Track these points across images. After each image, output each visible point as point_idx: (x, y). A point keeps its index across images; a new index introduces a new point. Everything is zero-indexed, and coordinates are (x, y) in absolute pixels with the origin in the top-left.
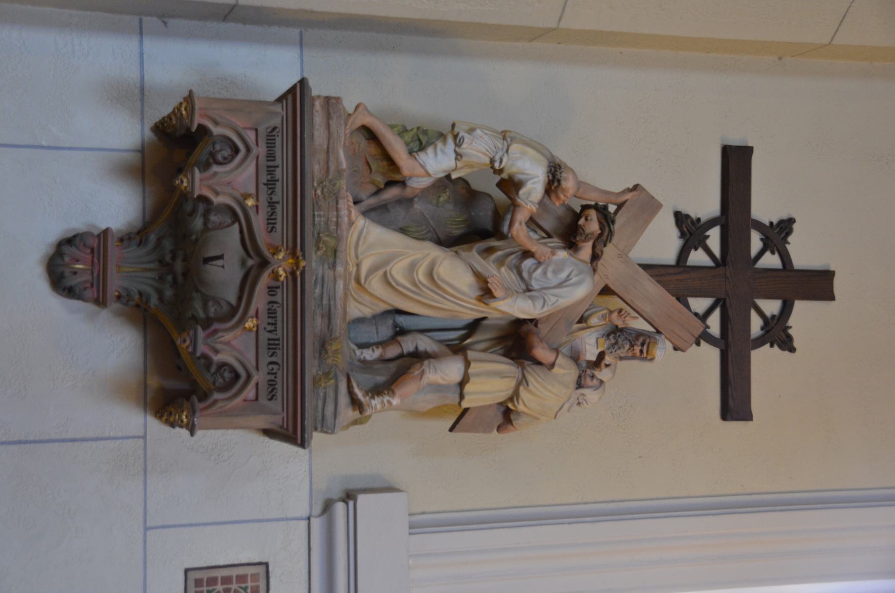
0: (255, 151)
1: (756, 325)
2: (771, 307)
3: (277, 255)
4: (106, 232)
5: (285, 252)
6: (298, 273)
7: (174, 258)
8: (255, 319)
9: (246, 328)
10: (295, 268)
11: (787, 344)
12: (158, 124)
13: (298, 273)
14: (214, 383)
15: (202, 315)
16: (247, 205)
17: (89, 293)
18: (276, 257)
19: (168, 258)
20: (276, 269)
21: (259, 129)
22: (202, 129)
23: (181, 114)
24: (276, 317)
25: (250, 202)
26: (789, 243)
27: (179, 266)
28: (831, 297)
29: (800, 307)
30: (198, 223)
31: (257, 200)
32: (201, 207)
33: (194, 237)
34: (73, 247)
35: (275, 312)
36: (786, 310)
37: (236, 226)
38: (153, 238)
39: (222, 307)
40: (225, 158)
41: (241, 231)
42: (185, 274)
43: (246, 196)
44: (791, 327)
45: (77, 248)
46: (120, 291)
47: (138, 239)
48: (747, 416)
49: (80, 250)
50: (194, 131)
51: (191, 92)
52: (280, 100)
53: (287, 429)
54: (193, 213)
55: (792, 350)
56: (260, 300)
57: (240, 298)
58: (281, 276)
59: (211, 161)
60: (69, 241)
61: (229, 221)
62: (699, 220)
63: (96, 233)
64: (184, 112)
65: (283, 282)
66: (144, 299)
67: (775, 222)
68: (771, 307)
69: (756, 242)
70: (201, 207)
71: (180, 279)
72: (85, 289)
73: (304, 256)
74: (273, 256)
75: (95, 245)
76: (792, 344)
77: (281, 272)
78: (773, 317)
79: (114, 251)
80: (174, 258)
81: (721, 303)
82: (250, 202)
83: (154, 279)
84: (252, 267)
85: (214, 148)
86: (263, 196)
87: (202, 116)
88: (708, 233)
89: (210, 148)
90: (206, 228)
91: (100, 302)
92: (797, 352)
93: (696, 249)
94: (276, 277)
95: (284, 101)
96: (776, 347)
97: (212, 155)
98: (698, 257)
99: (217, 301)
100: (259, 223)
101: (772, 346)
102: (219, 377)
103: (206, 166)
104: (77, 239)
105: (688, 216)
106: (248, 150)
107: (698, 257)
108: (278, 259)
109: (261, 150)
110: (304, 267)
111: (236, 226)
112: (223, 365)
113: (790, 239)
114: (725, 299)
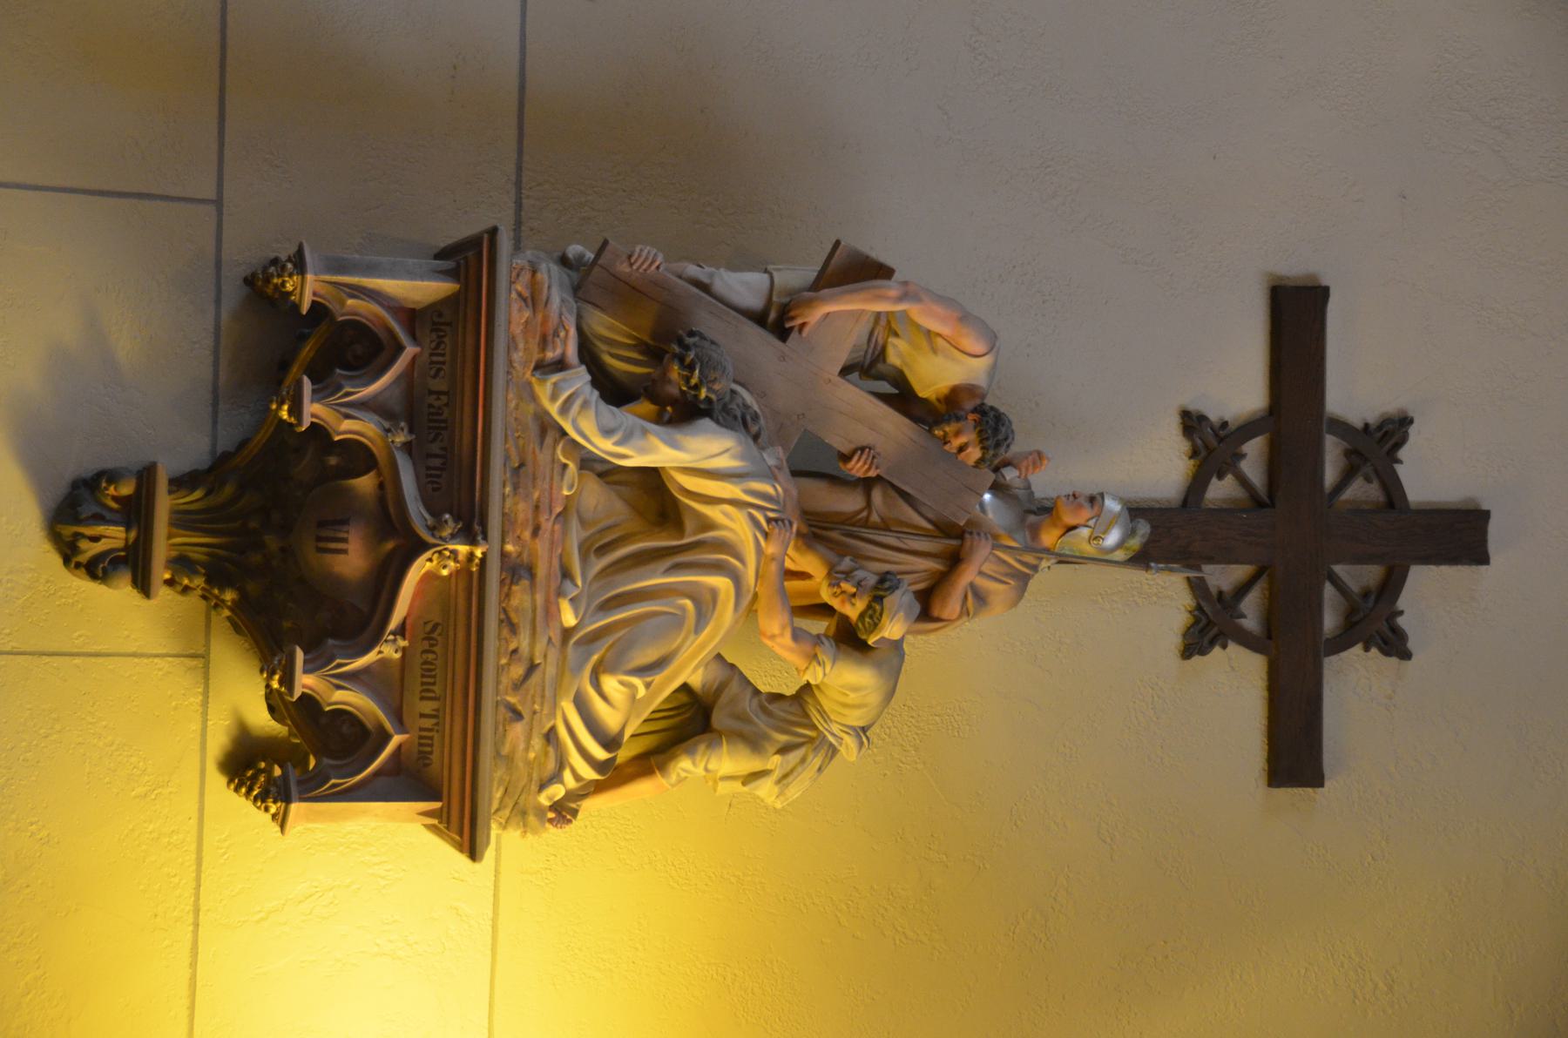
11: (1394, 644)
28: (1481, 558)
31: (411, 431)
44: (1401, 613)
50: (304, 313)
55: (1406, 655)
62: (1225, 424)
76: (1405, 645)
92: (1413, 659)
93: (1220, 477)
96: (1374, 651)
98: (1221, 490)
101: (1367, 649)
105: (1202, 418)
113: (1403, 453)
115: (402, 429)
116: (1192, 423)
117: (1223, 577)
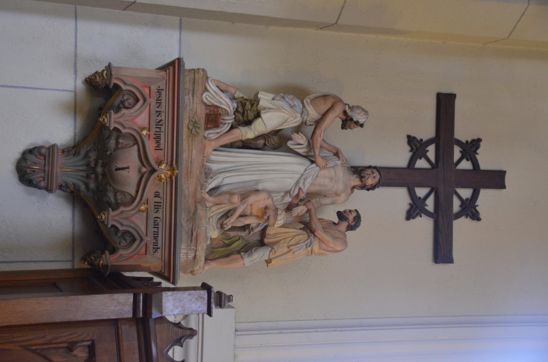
0: (149, 100)
1: (456, 205)
2: (466, 193)
3: (161, 166)
4: (54, 146)
5: (165, 164)
6: (174, 178)
7: (96, 164)
8: (146, 205)
9: (140, 210)
10: (172, 174)
11: (475, 216)
12: (87, 79)
13: (174, 178)
14: (120, 243)
15: (113, 200)
16: (143, 134)
17: (43, 184)
18: (160, 167)
19: (92, 165)
20: (160, 174)
21: (151, 87)
22: (117, 86)
23: (104, 77)
24: (158, 228)
25: (145, 132)
26: (478, 154)
27: (99, 170)
28: (503, 186)
29: (484, 194)
30: (112, 143)
32: (114, 134)
33: (108, 153)
34: (33, 155)
35: (158, 224)
36: (475, 195)
37: (135, 147)
38: (83, 152)
39: (126, 196)
40: (130, 104)
41: (139, 150)
42: (104, 175)
43: (144, 129)
44: (478, 206)
45: (36, 156)
46: (62, 184)
47: (73, 151)
48: (449, 260)
49: (38, 158)
51: (110, 65)
52: (164, 68)
53: (164, 273)
54: (109, 137)
55: (479, 219)
56: (149, 193)
57: (137, 192)
58: (163, 179)
59: (121, 106)
60: (30, 151)
61: (131, 143)
62: (422, 140)
63: (47, 146)
64: (105, 76)
65: (164, 183)
66: (76, 188)
67: (469, 141)
68: (466, 193)
69: (457, 153)
70: (114, 134)
71: (100, 178)
72: (40, 181)
73: (177, 167)
74: (158, 167)
75: (47, 155)
77: (163, 176)
78: (467, 199)
79: (60, 160)
80: (96, 164)
81: (435, 191)
82: (145, 132)
83: (83, 176)
84: (145, 173)
85: (123, 98)
86: (154, 129)
87: (115, 122)
88: (428, 149)
89: (120, 98)
90: (117, 148)
91: (49, 189)
93: (420, 159)
94: (160, 180)
95: (168, 70)
97: (122, 102)
98: (421, 164)
99: (124, 193)
100: (150, 145)
102: (123, 239)
103: (118, 110)
104: (36, 150)
105: (415, 138)
106: (145, 100)
107: (421, 164)
108: (161, 168)
109: (152, 101)
110: (177, 174)
111: (135, 147)
112: (126, 232)
113: (478, 151)
114: (437, 189)
115: (147, 130)
116: (411, 140)
117: (421, 192)
